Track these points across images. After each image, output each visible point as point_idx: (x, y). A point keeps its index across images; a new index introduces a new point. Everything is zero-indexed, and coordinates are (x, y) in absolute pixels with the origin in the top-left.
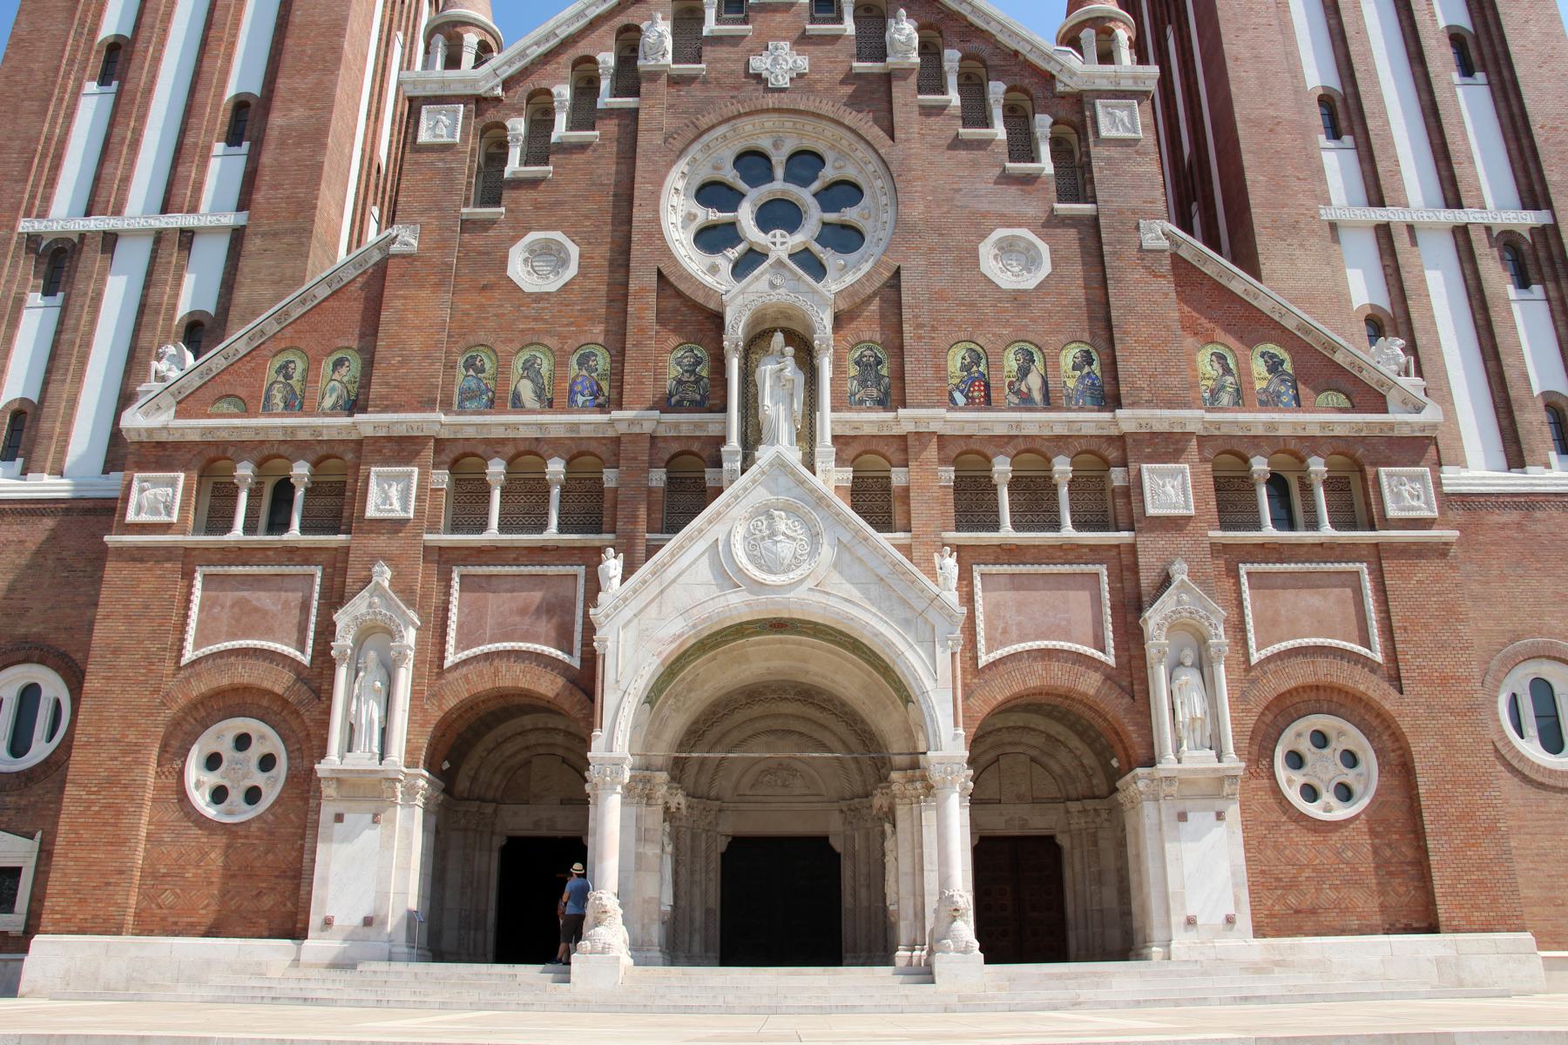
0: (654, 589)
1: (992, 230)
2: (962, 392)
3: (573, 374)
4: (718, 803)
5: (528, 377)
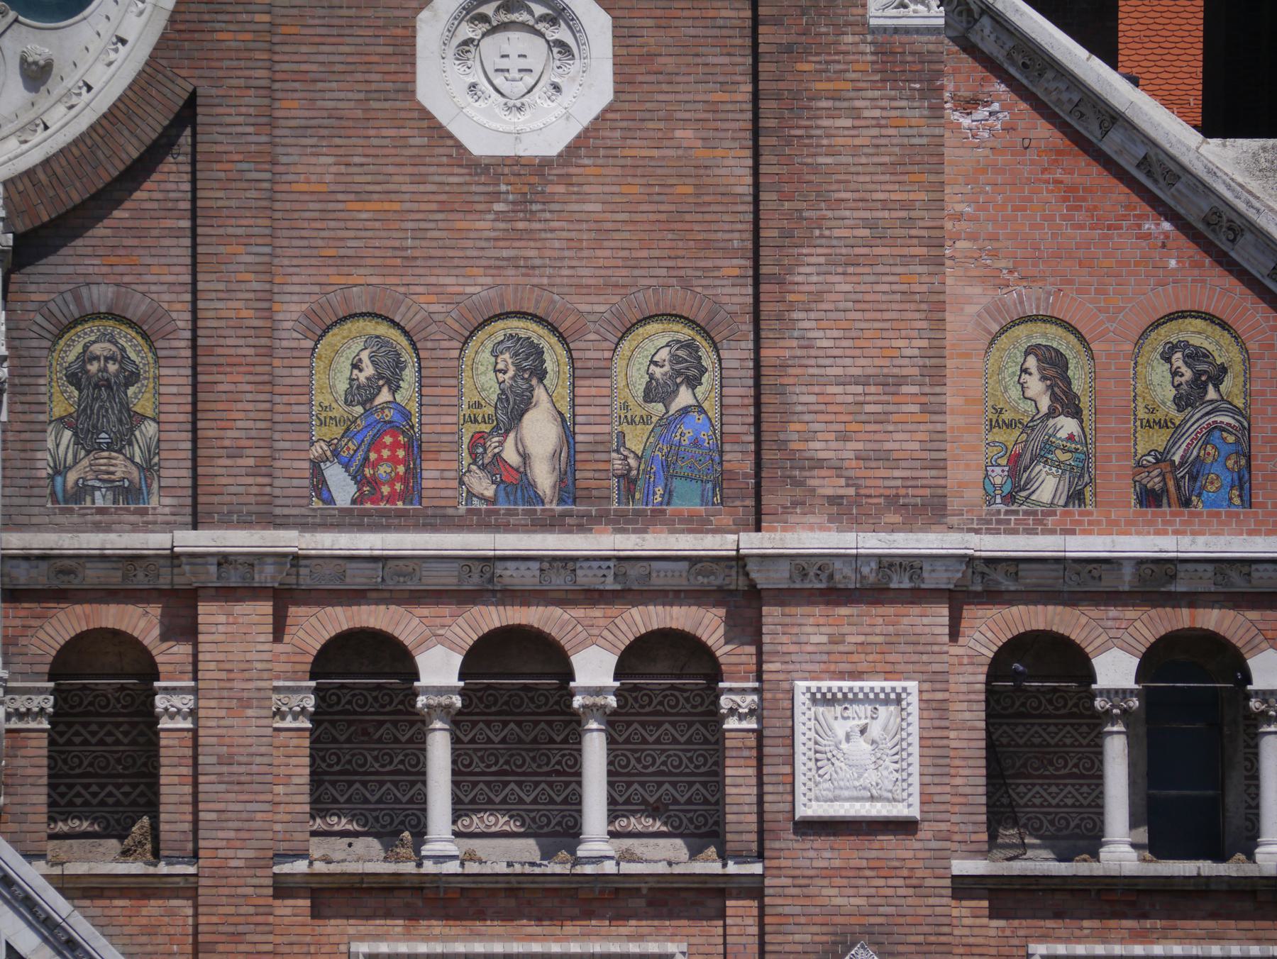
2: (346, 466)
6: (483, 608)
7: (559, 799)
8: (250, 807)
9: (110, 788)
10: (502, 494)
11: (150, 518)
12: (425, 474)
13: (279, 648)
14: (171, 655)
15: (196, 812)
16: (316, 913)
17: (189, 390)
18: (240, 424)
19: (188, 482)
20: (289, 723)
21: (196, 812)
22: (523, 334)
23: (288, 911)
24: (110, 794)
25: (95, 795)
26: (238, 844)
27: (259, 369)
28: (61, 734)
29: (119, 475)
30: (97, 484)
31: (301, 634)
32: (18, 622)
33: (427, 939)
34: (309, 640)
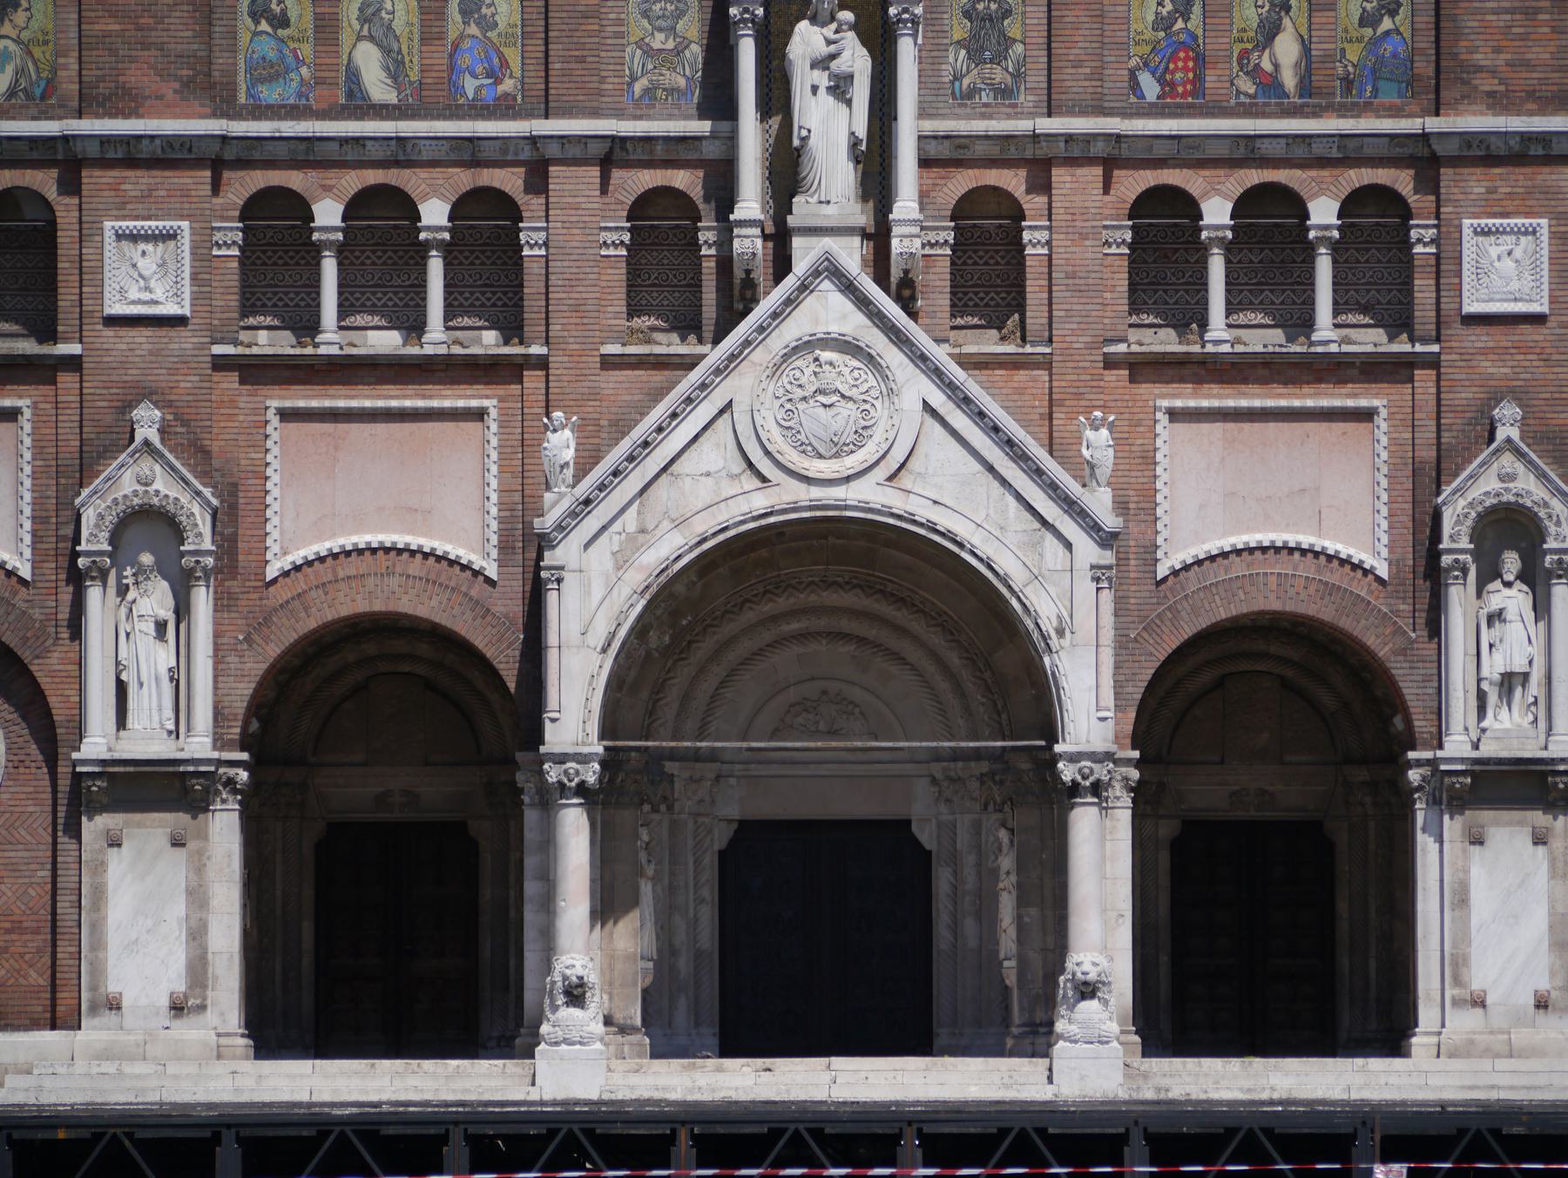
2: (1153, 74)
3: (452, 35)
5: (371, 38)
6: (1247, 171)
8: (1088, 307)
9: (992, 294)
10: (1260, 92)
11: (1019, 110)
12: (1207, 78)
13: (1107, 198)
14: (1033, 204)
15: (1050, 311)
16: (1132, 380)
17: (1045, 21)
18: (1080, 45)
19: (1045, 85)
20: (1114, 250)
21: (1050, 311)
23: (1114, 378)
24: (992, 299)
25: (982, 299)
26: (1080, 332)
28: (959, 258)
29: (998, 80)
30: (983, 86)
32: (930, 181)
33: (1208, 397)
34: (1128, 193)
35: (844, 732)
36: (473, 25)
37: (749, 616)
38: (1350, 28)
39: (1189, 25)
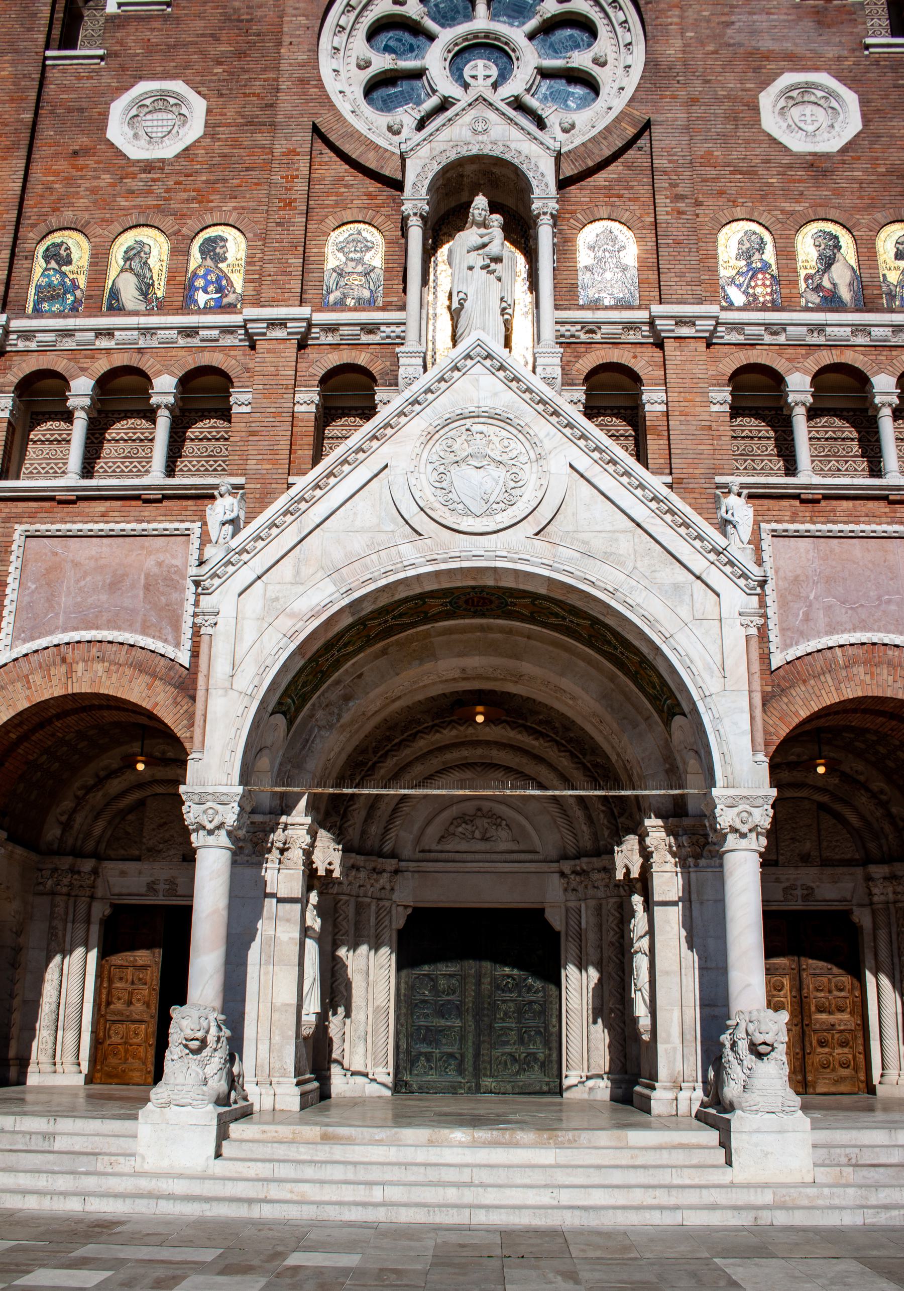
0: (289, 537)
1: (779, 75)
2: (739, 286)
4: (394, 861)
7: (860, 469)
22: (827, 230)
27: (690, 238)
31: (721, 365)
35: (493, 839)
36: (209, 260)
37: (422, 744)
38: (888, 261)
39: (764, 257)
